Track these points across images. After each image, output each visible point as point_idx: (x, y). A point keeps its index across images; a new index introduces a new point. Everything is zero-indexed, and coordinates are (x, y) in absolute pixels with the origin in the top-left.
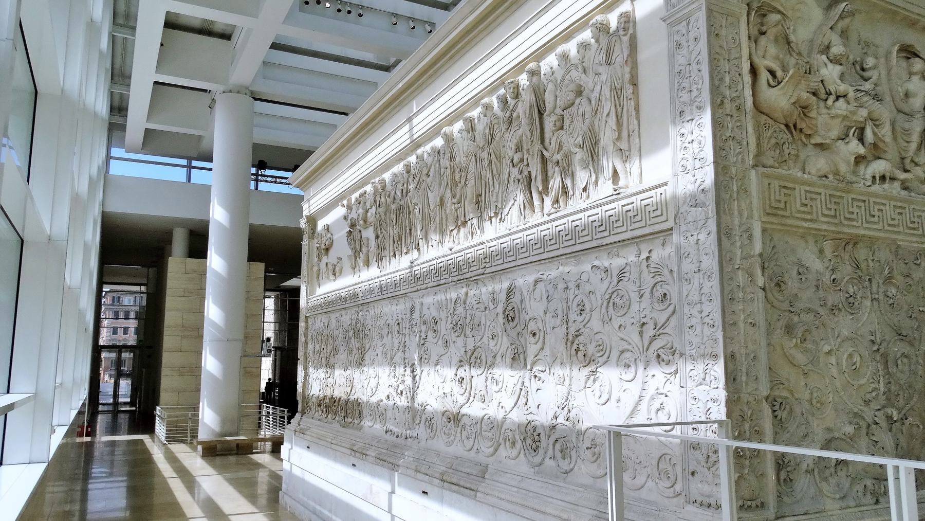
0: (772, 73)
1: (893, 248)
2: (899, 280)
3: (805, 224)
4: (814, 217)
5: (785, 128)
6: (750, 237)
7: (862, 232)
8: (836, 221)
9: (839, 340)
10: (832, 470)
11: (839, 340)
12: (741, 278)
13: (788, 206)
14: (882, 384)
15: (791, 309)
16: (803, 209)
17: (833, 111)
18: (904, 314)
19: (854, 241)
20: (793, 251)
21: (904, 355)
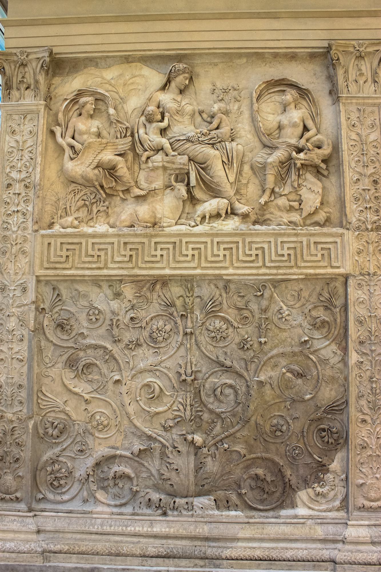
0: (72, 147)
1: (221, 284)
2: (231, 315)
3: (87, 272)
4: (102, 265)
5: (95, 191)
6: (25, 290)
7: (167, 272)
8: (130, 265)
9: (133, 372)
10: (111, 483)
11: (133, 372)
12: (12, 323)
13: (71, 259)
14: (188, 413)
15: (74, 346)
16: (90, 259)
17: (150, 164)
18: (234, 346)
19: (164, 281)
20: (85, 296)
21: (231, 386)
